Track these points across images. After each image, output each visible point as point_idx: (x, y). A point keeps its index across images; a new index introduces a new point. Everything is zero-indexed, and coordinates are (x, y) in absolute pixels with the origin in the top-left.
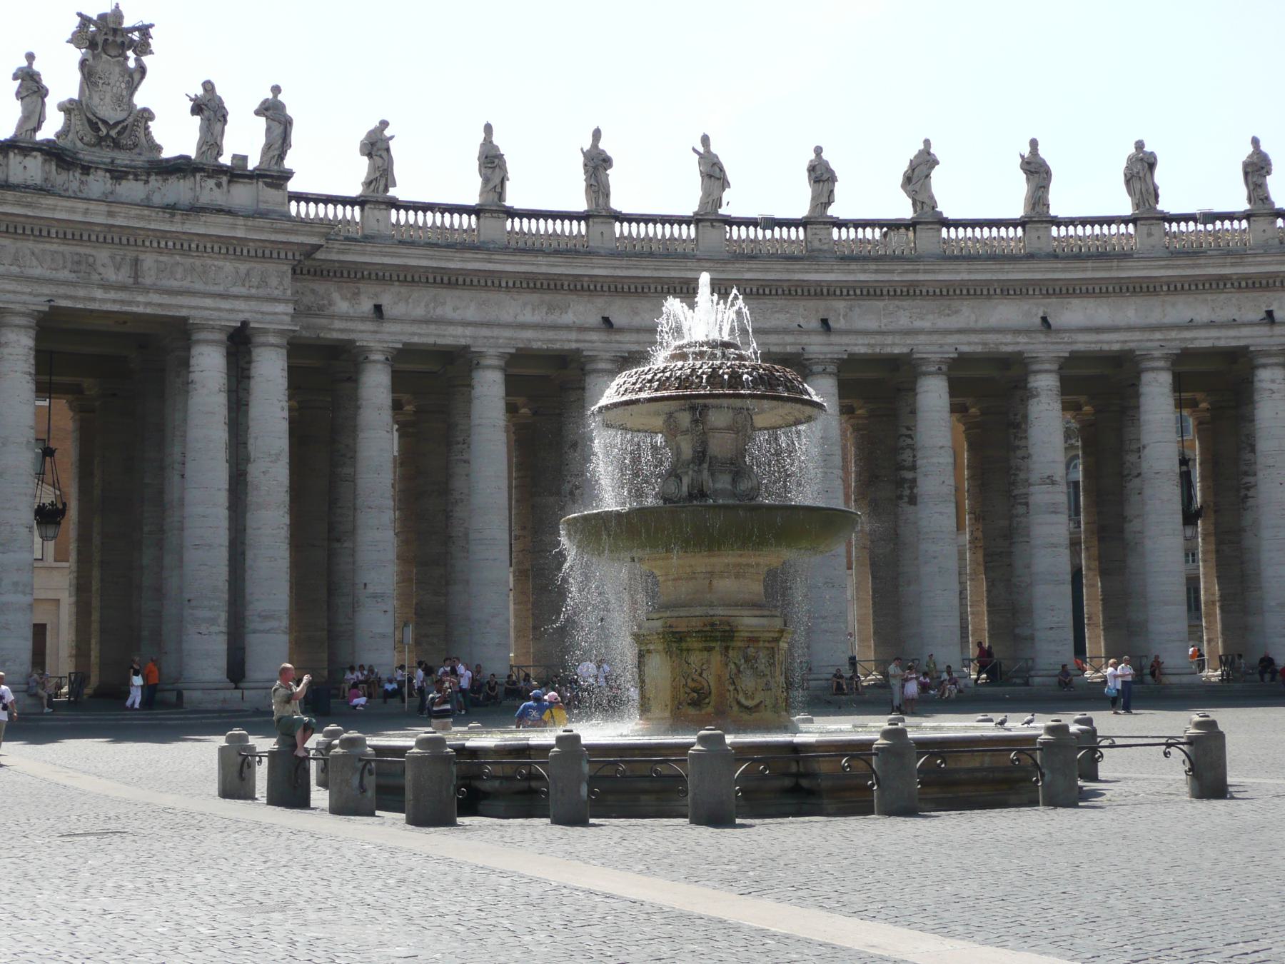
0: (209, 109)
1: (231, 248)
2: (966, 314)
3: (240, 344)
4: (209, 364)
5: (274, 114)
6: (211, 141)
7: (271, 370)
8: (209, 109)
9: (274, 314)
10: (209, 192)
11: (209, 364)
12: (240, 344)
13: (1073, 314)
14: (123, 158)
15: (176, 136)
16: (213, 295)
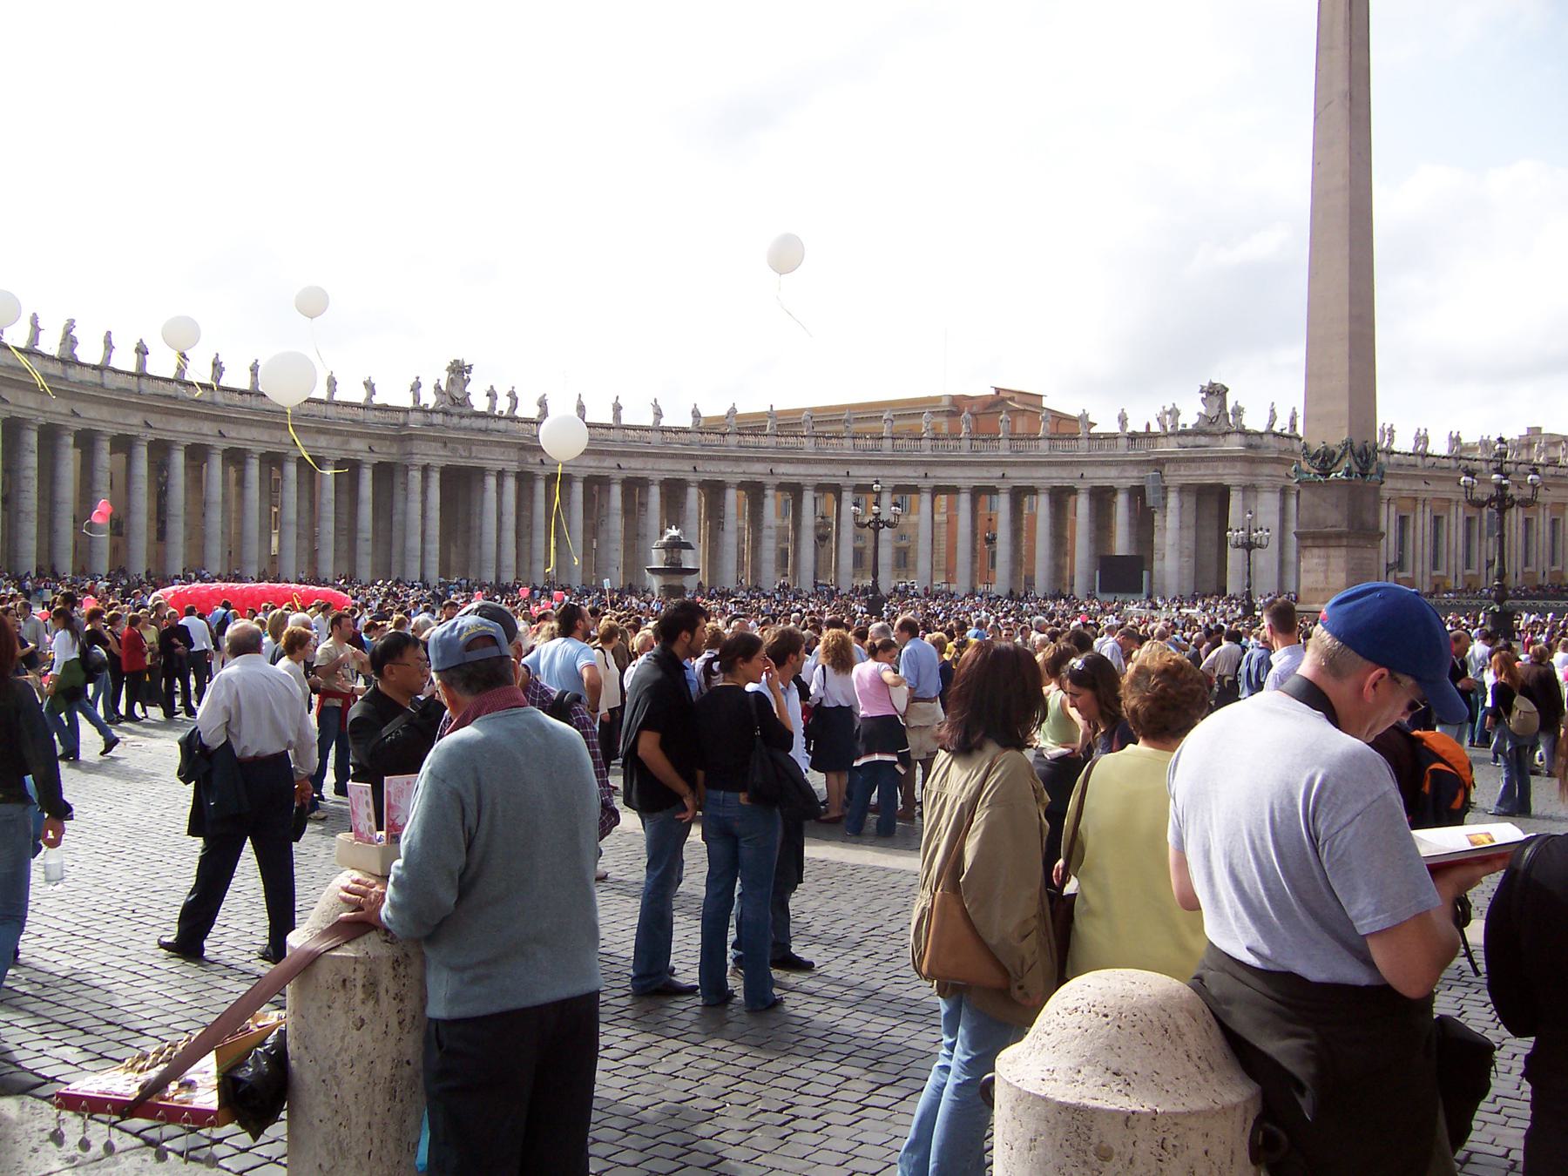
0: (492, 395)
1: (499, 444)
2: (744, 467)
3: (501, 475)
4: (491, 482)
5: (512, 395)
6: (492, 407)
7: (510, 484)
8: (492, 395)
9: (513, 467)
10: (492, 425)
11: (491, 482)
12: (501, 475)
13: (781, 469)
14: (465, 411)
15: (480, 403)
16: (493, 460)
